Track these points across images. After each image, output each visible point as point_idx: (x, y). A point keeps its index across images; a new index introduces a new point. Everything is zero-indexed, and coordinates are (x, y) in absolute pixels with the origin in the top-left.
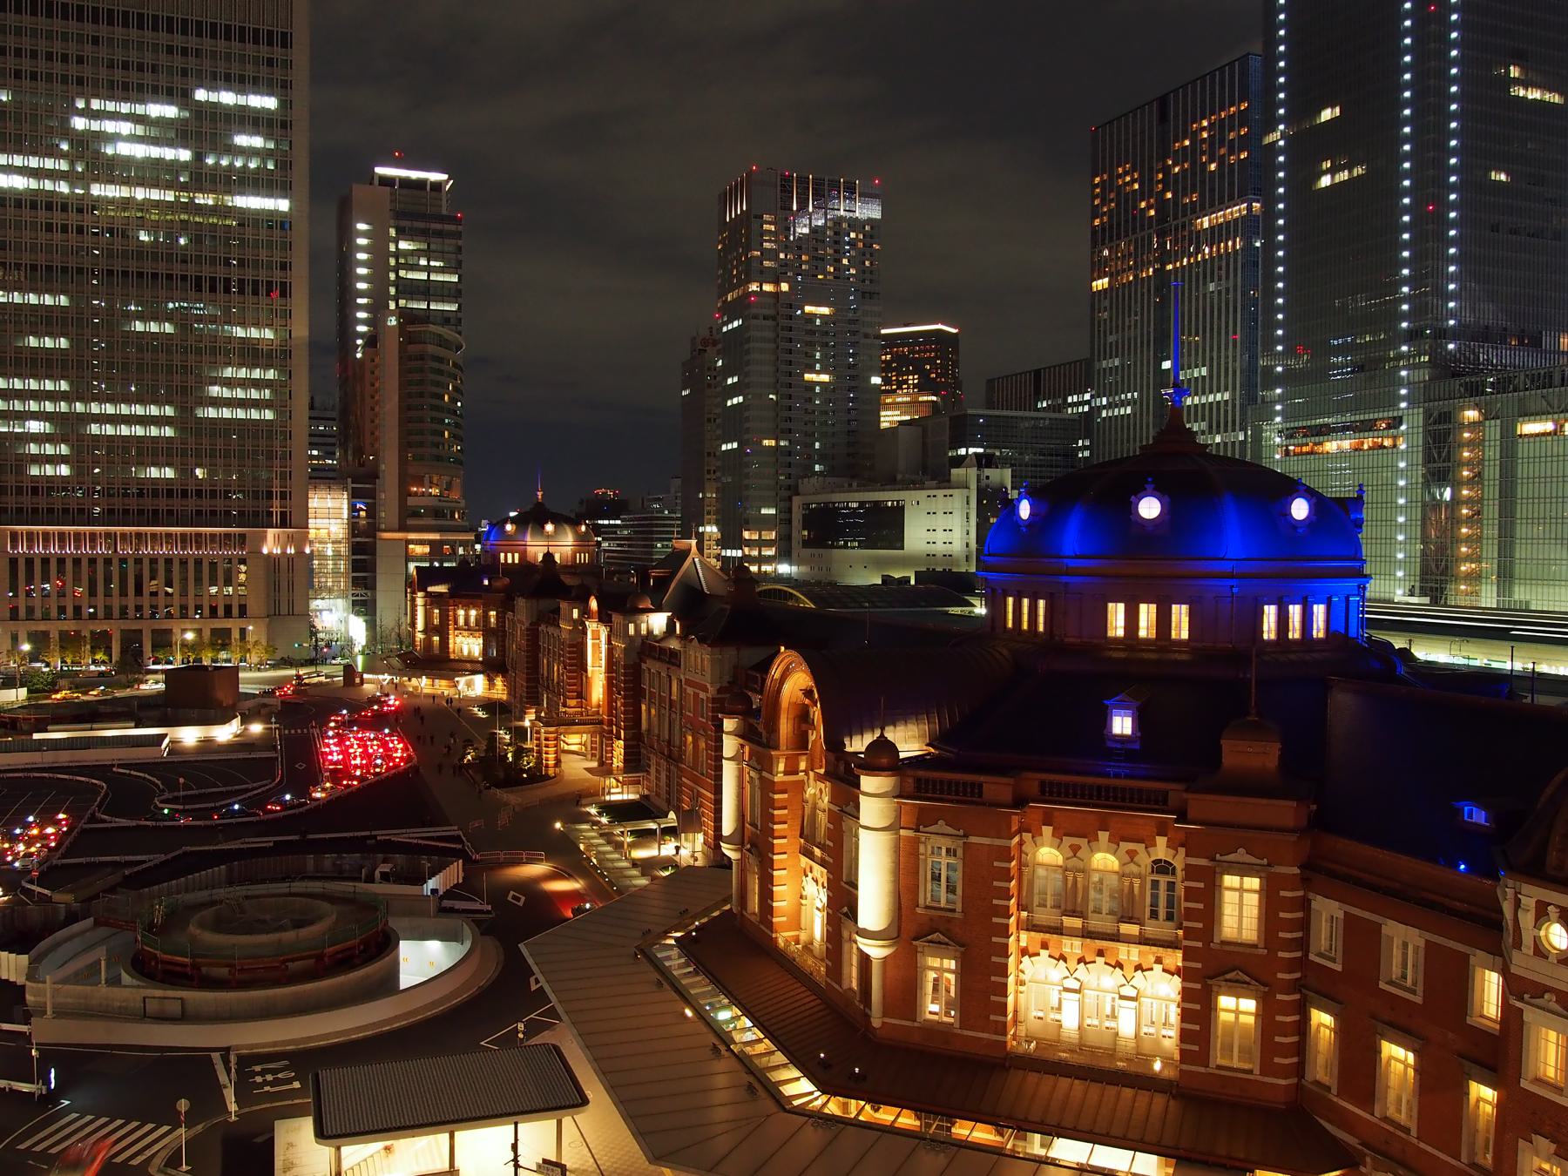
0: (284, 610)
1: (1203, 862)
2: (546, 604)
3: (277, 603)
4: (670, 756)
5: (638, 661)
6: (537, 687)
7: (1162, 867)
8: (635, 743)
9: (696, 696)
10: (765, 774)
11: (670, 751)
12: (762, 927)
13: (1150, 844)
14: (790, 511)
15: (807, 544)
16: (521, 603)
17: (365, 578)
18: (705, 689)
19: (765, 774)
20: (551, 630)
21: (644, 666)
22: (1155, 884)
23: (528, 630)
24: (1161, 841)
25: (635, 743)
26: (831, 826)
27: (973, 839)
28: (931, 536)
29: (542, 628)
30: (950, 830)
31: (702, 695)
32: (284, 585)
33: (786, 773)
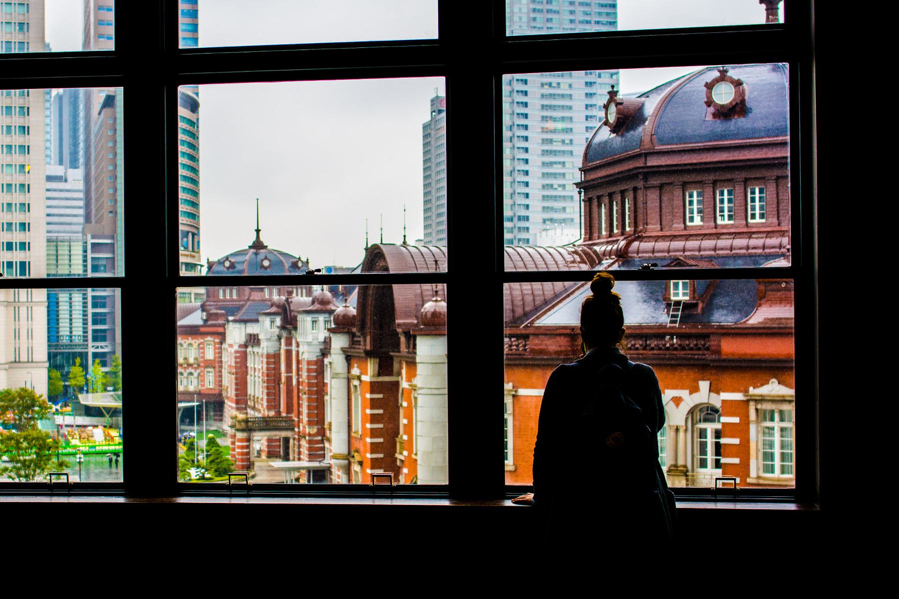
0: (24, 358)
1: (738, 396)
3: (17, 351)
5: (321, 357)
7: (710, 413)
8: (319, 438)
13: (694, 389)
17: (104, 331)
22: (703, 433)
23: (236, 352)
24: (704, 385)
25: (319, 438)
27: (522, 392)
29: (249, 349)
32: (24, 333)
33: (379, 375)
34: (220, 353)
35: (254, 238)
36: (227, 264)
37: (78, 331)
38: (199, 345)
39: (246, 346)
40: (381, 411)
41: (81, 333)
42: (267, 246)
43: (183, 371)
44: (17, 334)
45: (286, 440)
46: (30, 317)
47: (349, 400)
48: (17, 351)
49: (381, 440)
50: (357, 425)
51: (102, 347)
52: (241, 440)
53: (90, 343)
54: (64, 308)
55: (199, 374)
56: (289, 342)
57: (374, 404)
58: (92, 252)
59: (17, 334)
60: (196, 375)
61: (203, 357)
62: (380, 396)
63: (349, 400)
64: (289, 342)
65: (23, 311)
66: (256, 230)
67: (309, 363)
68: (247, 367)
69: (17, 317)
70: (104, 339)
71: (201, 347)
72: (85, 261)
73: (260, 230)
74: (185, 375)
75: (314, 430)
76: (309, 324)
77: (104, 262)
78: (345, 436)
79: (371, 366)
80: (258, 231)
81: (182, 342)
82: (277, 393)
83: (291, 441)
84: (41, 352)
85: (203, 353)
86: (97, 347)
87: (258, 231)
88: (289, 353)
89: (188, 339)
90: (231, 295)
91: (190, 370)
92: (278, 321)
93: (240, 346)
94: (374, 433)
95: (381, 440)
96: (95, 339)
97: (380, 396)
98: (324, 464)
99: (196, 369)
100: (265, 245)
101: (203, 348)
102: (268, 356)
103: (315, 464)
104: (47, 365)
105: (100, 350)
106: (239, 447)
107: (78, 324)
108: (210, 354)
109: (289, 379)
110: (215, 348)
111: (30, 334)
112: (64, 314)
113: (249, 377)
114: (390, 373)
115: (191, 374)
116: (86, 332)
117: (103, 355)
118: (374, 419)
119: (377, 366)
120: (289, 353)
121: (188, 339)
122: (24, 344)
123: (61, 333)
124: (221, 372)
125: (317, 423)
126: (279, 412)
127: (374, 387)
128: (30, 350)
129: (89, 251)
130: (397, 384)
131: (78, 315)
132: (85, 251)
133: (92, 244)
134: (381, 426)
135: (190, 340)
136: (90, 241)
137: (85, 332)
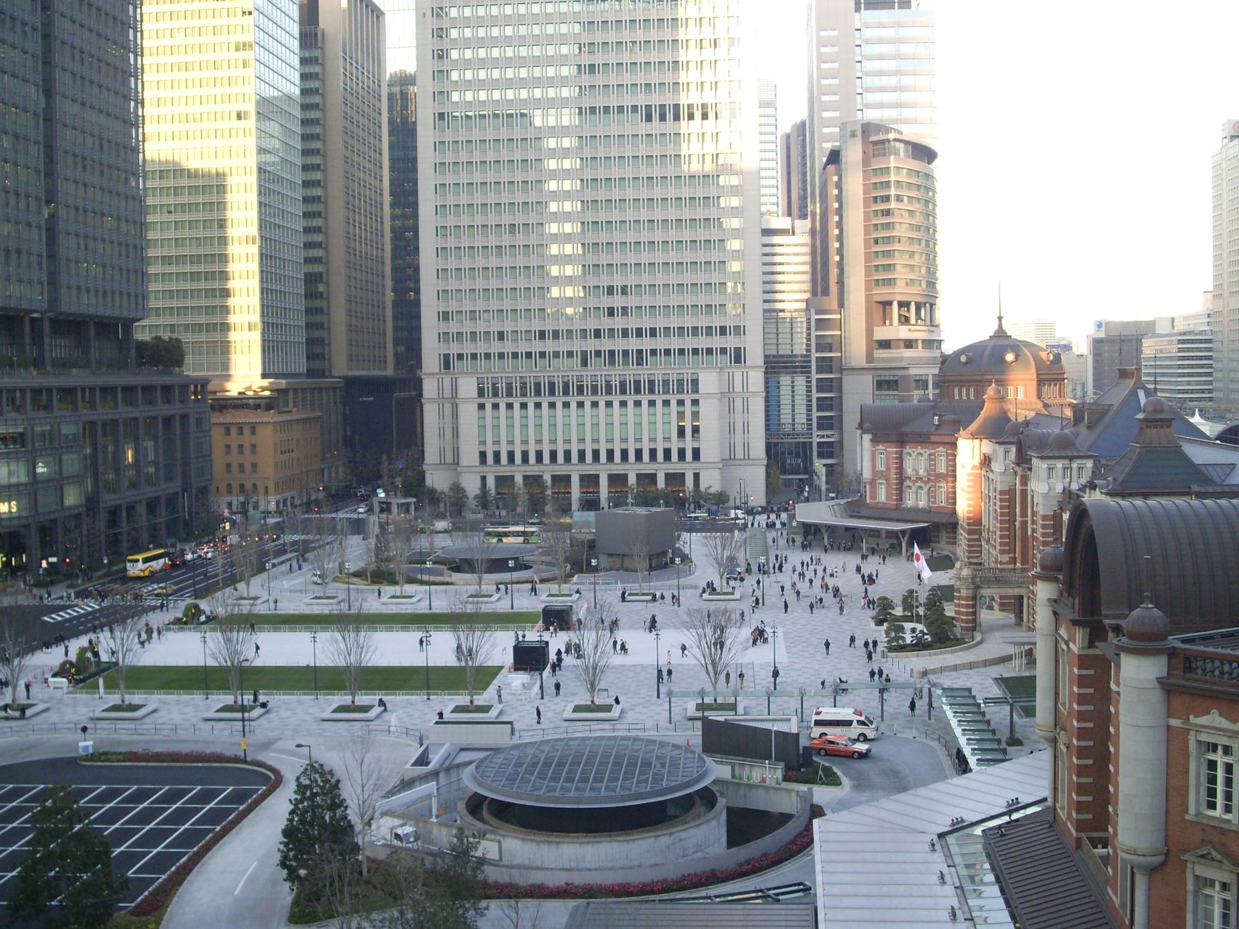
0: (739, 455)
3: (732, 448)
5: (1059, 511)
6: (979, 540)
12: (1069, 824)
23: (970, 475)
30: (1225, 724)
32: (739, 427)
33: (1091, 645)
35: (996, 327)
36: (963, 358)
37: (801, 418)
38: (930, 455)
40: (1091, 691)
41: (804, 421)
43: (911, 484)
44: (731, 429)
45: (1021, 597)
46: (746, 409)
47: (1057, 661)
48: (732, 448)
49: (1091, 725)
50: (1064, 694)
51: (828, 436)
52: (967, 599)
53: (815, 432)
54: (785, 392)
59: (731, 429)
60: (926, 489)
61: (935, 470)
62: (1091, 672)
63: (1057, 661)
65: (738, 403)
67: (1044, 518)
69: (731, 409)
71: (932, 459)
72: (809, 339)
74: (914, 489)
76: (1044, 473)
78: (1050, 703)
80: (1000, 318)
81: (911, 451)
82: (1013, 535)
84: (758, 449)
85: (935, 465)
86: (823, 436)
87: (1000, 318)
91: (919, 484)
94: (1081, 716)
95: (1091, 725)
96: (820, 427)
97: (1091, 672)
99: (926, 483)
101: (934, 460)
102: (1002, 493)
104: (765, 462)
107: (801, 409)
109: (1024, 524)
110: (948, 461)
111: (746, 428)
112: (785, 399)
115: (921, 488)
118: (1082, 699)
120: (1024, 493)
122: (739, 438)
123: (782, 421)
127: (1083, 661)
128: (746, 446)
129: (813, 329)
131: (801, 401)
132: (809, 329)
134: (1091, 708)
135: (919, 450)
137: (809, 420)
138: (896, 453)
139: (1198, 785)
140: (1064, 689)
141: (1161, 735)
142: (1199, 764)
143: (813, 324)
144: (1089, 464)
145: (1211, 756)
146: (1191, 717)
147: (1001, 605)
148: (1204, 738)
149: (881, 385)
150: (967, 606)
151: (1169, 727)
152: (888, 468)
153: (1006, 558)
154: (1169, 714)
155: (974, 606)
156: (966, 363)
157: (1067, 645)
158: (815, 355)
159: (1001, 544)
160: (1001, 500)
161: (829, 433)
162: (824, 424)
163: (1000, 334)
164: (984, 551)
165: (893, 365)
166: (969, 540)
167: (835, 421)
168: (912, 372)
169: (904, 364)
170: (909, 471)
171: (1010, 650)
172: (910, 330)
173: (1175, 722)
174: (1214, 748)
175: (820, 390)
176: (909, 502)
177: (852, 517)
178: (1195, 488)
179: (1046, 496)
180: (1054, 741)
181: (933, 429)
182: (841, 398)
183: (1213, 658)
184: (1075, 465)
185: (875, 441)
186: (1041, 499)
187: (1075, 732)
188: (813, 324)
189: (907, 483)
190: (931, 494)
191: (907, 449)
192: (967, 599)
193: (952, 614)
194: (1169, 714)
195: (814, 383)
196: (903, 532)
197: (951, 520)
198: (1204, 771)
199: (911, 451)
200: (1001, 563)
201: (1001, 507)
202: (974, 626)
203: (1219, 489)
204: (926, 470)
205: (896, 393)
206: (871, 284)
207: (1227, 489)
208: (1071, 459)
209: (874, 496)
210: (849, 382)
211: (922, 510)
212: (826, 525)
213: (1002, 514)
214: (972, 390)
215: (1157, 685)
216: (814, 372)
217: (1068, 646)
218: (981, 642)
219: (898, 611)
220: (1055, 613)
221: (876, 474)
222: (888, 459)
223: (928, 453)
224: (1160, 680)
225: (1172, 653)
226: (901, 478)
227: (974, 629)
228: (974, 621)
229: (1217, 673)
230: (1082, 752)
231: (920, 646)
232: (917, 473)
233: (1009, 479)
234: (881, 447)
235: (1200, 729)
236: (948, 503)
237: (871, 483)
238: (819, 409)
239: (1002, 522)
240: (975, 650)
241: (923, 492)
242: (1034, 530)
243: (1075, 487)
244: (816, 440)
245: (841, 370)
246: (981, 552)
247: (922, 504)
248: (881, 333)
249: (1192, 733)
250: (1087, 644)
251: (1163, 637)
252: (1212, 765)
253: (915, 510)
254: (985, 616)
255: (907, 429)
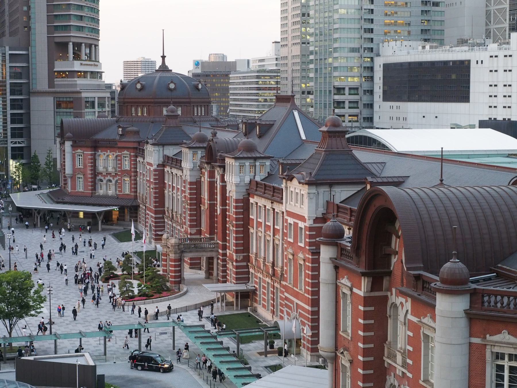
2: (171, 151)
4: (274, 274)
5: (247, 196)
6: (163, 218)
8: (245, 264)
9: (296, 224)
10: (355, 290)
11: (274, 270)
14: (372, 69)
15: (387, 97)
16: (149, 148)
17: (21, 128)
18: (302, 218)
19: (355, 290)
20: (175, 171)
21: (252, 200)
23: (155, 170)
25: (245, 264)
26: (411, 334)
28: (493, 91)
31: (301, 224)
33: (372, 290)
34: (136, 164)
36: (139, 86)
38: (117, 156)
39: (163, 165)
40: (372, 322)
42: (171, 70)
43: (102, 178)
47: (337, 302)
49: (372, 346)
50: (345, 326)
51: (19, 143)
52: (175, 261)
53: (10, 140)
55: (116, 181)
56: (212, 175)
57: (366, 315)
58: (10, 62)
60: (114, 182)
61: (121, 168)
62: (372, 308)
63: (337, 302)
64: (212, 175)
66: (162, 57)
67: (237, 201)
68: (164, 183)
70: (21, 136)
73: (165, 57)
74: (105, 181)
75: (241, 256)
76: (236, 169)
77: (19, 70)
78: (332, 332)
79: (365, 283)
80: (163, 57)
82: (199, 214)
83: (215, 261)
85: (121, 164)
86: (16, 143)
87: (163, 57)
88: (212, 185)
89: (107, 152)
90: (142, 113)
91: (109, 178)
92: (200, 153)
93: (158, 166)
94: (365, 340)
95: (372, 346)
96: (13, 136)
97: (372, 308)
98: (250, 286)
99: (113, 177)
100: (170, 69)
101: (120, 160)
102: (191, 183)
103: (242, 287)
105: (17, 145)
106: (171, 266)
108: (127, 165)
109: (212, 208)
110: (131, 161)
113: (166, 192)
114: (381, 290)
115: (110, 181)
116: (6, 130)
117: (21, 149)
119: (370, 284)
120: (212, 185)
121: (107, 152)
124: (136, 180)
125: (243, 251)
126: (199, 232)
127: (367, 301)
129: (8, 61)
130: (386, 298)
133: (11, 55)
134: (372, 334)
136: (8, 52)
138: (91, 155)
139: (492, 382)
140: (345, 321)
141: (465, 349)
142: (492, 368)
143: (7, 57)
144: (268, 163)
145: (500, 362)
146: (488, 336)
147: (191, 264)
148: (497, 350)
149: (58, 105)
150: (175, 266)
151: (470, 343)
152: (85, 166)
153: (194, 231)
154: (471, 335)
155: (180, 266)
156: (140, 90)
157: (351, 290)
158: (9, 81)
159: (191, 221)
160: (190, 189)
161: (20, 140)
162: (16, 133)
163: (164, 68)
164: (167, 226)
165: (70, 90)
166: (156, 218)
167: (24, 132)
168: (84, 95)
169: (78, 89)
170: (101, 168)
171: (213, 296)
172: (81, 64)
173: (476, 340)
174: (502, 356)
175: (13, 107)
176: (101, 192)
177: (58, 203)
178: (370, 179)
179: (237, 185)
180: (335, 359)
181: (118, 138)
182: (28, 114)
183: (496, 294)
184: (258, 164)
185: (74, 146)
186: (234, 188)
187: (361, 351)
188: (7, 57)
189: (100, 177)
190: (119, 185)
191: (100, 152)
192: (175, 261)
193: (161, 273)
194: (471, 335)
195: (8, 103)
196: (99, 213)
197: (134, 204)
198: (494, 373)
199: (102, 154)
200: (191, 234)
201: (190, 194)
202: (179, 280)
203: (379, 180)
204: (113, 168)
205: (72, 110)
206: (52, 29)
207: (385, 180)
208: (255, 159)
209: (74, 187)
210: (35, 102)
211: (112, 197)
212: (36, 209)
213: (191, 199)
214: (145, 109)
215: (464, 315)
216: (8, 94)
217: (351, 290)
218: (185, 293)
219: (119, 272)
220: (336, 268)
221: (75, 170)
222: (84, 159)
223: (115, 154)
224: (466, 311)
225: (473, 293)
226: (95, 173)
227: (179, 282)
228: (180, 276)
229: (499, 305)
230: (366, 366)
231: (144, 296)
232: (107, 170)
233: (196, 174)
234: (79, 151)
235: (494, 344)
236: (131, 191)
237: (71, 178)
238: (12, 122)
239: (191, 204)
240: (184, 297)
241: (112, 185)
242: (224, 212)
243: (258, 179)
244: (10, 145)
245: (29, 93)
246: (164, 226)
247: (111, 193)
248: (60, 66)
249: (488, 347)
250: (370, 289)
251: (464, 282)
252: (500, 368)
253: (106, 197)
254: (188, 273)
255: (100, 136)
